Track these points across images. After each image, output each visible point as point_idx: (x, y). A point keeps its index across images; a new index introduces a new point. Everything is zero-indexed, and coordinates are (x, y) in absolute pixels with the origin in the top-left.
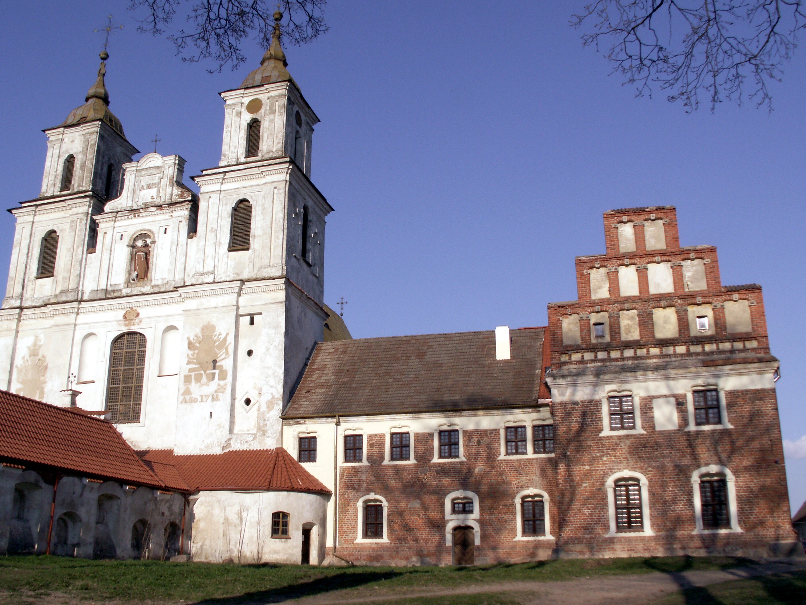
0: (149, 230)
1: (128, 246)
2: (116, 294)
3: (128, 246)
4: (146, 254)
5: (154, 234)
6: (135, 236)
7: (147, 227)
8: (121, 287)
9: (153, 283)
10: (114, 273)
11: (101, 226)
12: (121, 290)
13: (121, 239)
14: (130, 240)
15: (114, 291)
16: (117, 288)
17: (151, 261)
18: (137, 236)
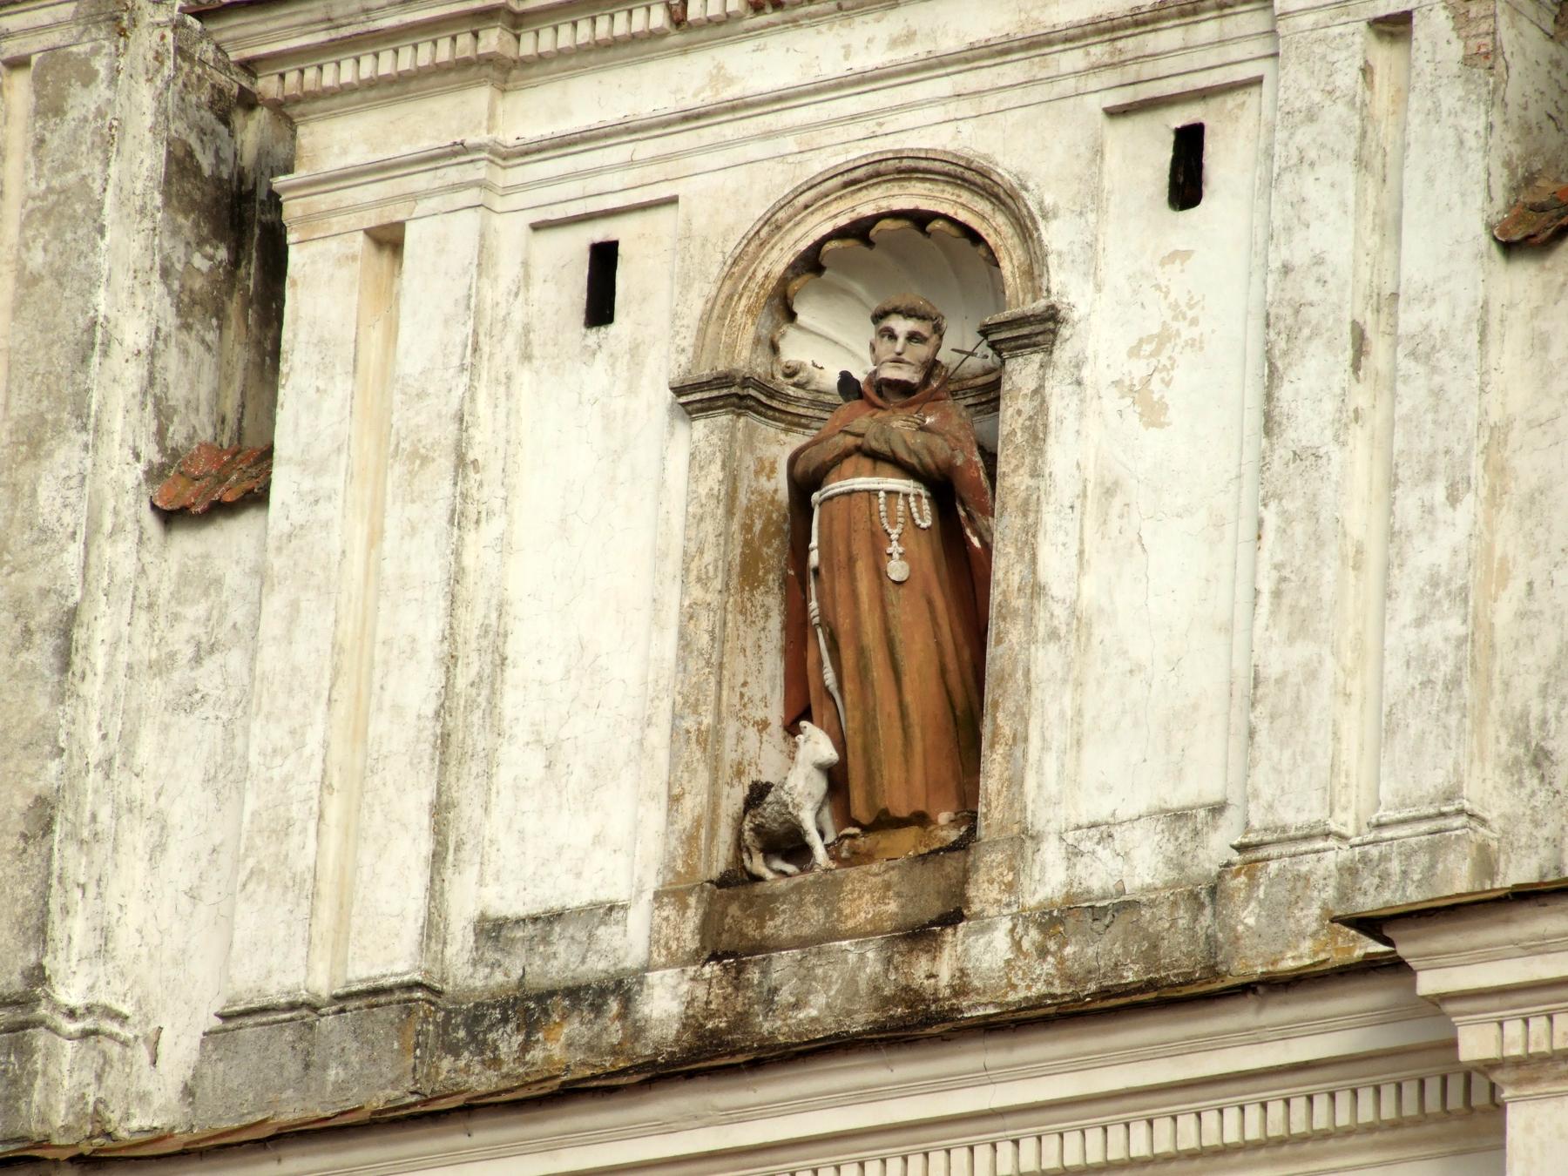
0: (970, 176)
1: (702, 395)
2: (562, 1046)
3: (707, 394)
4: (943, 488)
5: (1025, 229)
6: (779, 259)
7: (927, 123)
8: (629, 942)
9: (1049, 879)
10: (518, 761)
11: (333, 142)
12: (620, 989)
13: (600, 309)
14: (718, 312)
15: (529, 1008)
16: (563, 961)
17: (1006, 573)
18: (811, 262)
